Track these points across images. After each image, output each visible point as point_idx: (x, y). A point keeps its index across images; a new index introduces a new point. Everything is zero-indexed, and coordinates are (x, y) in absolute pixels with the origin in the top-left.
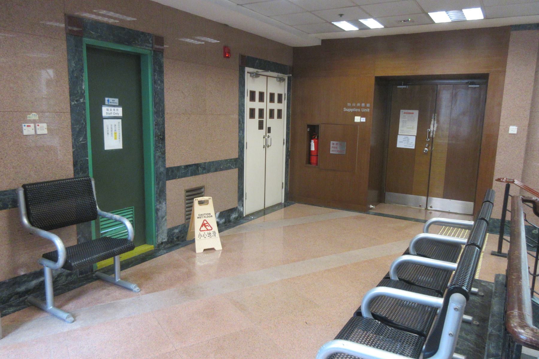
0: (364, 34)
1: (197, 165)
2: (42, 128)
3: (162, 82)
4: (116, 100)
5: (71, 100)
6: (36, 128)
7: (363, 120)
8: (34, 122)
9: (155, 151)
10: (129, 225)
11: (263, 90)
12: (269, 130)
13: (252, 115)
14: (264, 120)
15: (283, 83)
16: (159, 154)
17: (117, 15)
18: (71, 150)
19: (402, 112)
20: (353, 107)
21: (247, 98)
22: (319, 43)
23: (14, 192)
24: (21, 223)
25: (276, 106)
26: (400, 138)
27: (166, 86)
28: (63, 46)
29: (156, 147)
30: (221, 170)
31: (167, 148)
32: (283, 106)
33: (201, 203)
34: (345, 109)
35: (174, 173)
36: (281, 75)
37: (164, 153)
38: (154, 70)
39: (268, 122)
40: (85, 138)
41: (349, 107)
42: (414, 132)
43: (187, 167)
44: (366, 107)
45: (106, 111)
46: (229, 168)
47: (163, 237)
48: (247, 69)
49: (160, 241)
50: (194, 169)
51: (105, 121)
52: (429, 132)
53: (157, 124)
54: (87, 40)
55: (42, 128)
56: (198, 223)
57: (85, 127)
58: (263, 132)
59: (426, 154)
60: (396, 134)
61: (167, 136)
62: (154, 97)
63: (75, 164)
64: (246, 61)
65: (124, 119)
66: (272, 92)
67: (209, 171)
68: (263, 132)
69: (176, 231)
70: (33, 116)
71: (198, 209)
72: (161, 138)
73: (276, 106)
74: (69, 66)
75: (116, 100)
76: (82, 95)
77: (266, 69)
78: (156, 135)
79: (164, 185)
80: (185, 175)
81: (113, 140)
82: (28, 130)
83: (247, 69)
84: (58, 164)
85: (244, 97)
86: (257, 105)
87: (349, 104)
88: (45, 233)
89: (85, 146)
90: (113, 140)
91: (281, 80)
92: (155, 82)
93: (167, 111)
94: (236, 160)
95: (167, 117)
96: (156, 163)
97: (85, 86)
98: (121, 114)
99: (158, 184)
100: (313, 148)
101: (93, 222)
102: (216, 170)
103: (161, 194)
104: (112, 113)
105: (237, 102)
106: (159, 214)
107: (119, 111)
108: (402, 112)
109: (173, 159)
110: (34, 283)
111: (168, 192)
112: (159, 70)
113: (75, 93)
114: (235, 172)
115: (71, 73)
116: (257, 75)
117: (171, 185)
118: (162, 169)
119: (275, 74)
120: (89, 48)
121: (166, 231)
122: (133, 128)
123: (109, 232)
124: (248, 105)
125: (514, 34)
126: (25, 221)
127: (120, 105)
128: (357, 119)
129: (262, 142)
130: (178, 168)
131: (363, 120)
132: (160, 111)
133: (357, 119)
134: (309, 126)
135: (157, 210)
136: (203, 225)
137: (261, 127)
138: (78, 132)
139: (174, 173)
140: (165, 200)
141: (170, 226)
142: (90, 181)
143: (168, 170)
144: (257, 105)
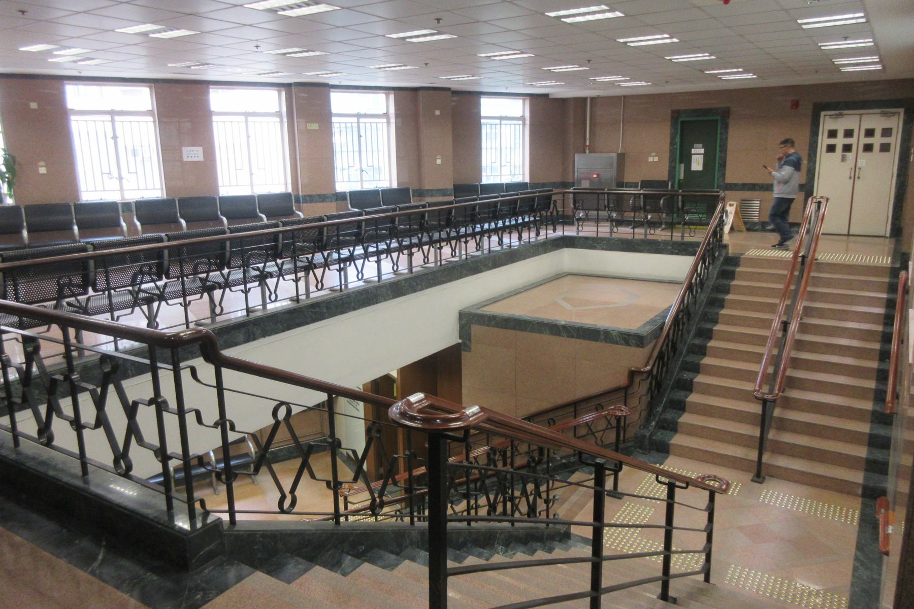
2: (656, 159)
3: (727, 133)
32: (895, 141)
37: (724, 174)
43: (744, 185)
45: (693, 151)
55: (656, 159)
64: (818, 109)
65: (705, 155)
70: (654, 154)
72: (723, 165)
76: (676, 144)
81: (697, 164)
82: (650, 159)
85: (817, 135)
90: (697, 164)
91: (884, 114)
92: (721, 134)
97: (678, 140)
107: (702, 151)
109: (730, 178)
112: (726, 126)
113: (672, 143)
116: (841, 115)
119: (879, 111)
124: (823, 141)
132: (724, 149)
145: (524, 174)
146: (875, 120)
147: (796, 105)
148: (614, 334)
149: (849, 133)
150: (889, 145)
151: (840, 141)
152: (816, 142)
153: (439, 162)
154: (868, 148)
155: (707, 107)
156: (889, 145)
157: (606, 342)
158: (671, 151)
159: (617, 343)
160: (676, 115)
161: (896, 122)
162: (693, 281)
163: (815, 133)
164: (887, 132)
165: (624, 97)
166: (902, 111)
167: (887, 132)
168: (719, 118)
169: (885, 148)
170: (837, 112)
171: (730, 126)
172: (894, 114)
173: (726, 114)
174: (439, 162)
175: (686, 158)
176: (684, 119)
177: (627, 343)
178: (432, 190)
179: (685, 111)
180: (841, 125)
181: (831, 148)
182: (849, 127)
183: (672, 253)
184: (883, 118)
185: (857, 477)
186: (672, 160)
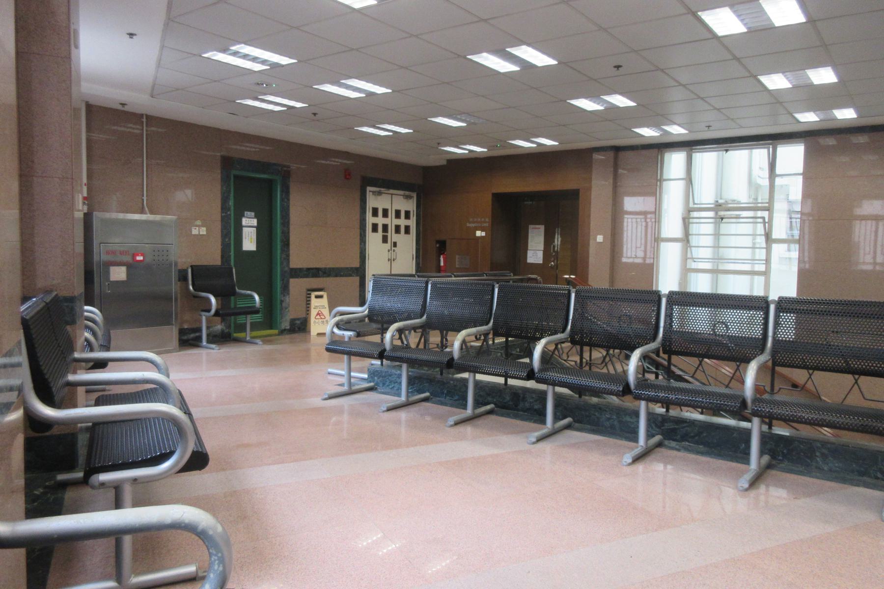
0: (472, 156)
1: (318, 269)
2: (203, 231)
3: (288, 200)
4: (253, 214)
5: (222, 212)
7: (483, 234)
8: (199, 226)
9: (282, 253)
10: (257, 297)
11: (388, 206)
12: (395, 244)
13: (375, 228)
14: (389, 234)
15: (411, 201)
16: (284, 256)
17: (257, 146)
18: (220, 247)
19: (531, 227)
20: (474, 222)
21: (369, 214)
22: (445, 163)
23: (186, 271)
24: (188, 288)
25: (402, 222)
26: (530, 254)
27: (291, 202)
28: (217, 175)
29: (283, 251)
30: (341, 276)
31: (291, 252)
32: (412, 223)
33: (317, 297)
34: (468, 225)
35: (298, 273)
36: (407, 193)
37: (288, 256)
38: (282, 191)
39: (392, 236)
40: (230, 239)
41: (470, 223)
42: (542, 247)
43: (308, 269)
44: (485, 222)
45: (245, 221)
46: (350, 275)
47: (286, 325)
48: (369, 189)
49: (283, 327)
50: (314, 272)
52: (554, 247)
53: (283, 232)
55: (203, 231)
56: (314, 312)
57: (231, 233)
58: (388, 246)
59: (552, 267)
60: (526, 249)
61: (291, 243)
62: (281, 211)
63: (222, 257)
64: (367, 181)
65: (259, 228)
66: (398, 208)
67: (329, 276)
68: (388, 246)
69: (298, 322)
70: (199, 223)
71: (314, 302)
72: (286, 244)
73: (402, 222)
74: (222, 189)
75: (253, 214)
76: (229, 209)
77: (389, 188)
78: (282, 241)
79: (288, 282)
80: (306, 276)
81: (249, 244)
82: (195, 231)
83: (369, 189)
84: (212, 257)
85: (365, 213)
86: (380, 220)
87: (471, 220)
88: (204, 294)
89: (229, 245)
90: (249, 244)
91: (408, 197)
93: (291, 222)
94: (357, 269)
95: (291, 227)
96: (282, 263)
97: (231, 203)
98: (256, 224)
99: (283, 280)
100: (442, 264)
101: (232, 298)
102: (336, 276)
103: (286, 288)
104: (249, 224)
105: (358, 217)
106: (284, 305)
107: (255, 222)
108: (531, 227)
109: (297, 261)
110: (192, 335)
111: (291, 288)
112: (286, 191)
113: (224, 208)
114: (357, 279)
115: (223, 194)
116: (380, 193)
117: (292, 281)
118: (286, 269)
120: (236, 177)
121: (289, 320)
122: (265, 234)
123: (241, 304)
124: (370, 220)
125: (597, 156)
126: (191, 288)
127: (256, 217)
128: (479, 233)
129: (386, 255)
130: (301, 269)
131: (483, 234)
132: (286, 223)
133: (479, 233)
134: (438, 242)
135: (282, 301)
136: (318, 314)
137: (385, 240)
138: (225, 235)
139: (298, 273)
140: (288, 294)
141: (292, 317)
142: (231, 269)
143: (292, 269)
144: (380, 220)
158: (223, 219)
160: (227, 163)
161: (410, 205)
162: (79, 425)
164: (407, 215)
166: (415, 195)
169: (407, 230)
171: (291, 190)
173: (286, 175)
181: (375, 228)
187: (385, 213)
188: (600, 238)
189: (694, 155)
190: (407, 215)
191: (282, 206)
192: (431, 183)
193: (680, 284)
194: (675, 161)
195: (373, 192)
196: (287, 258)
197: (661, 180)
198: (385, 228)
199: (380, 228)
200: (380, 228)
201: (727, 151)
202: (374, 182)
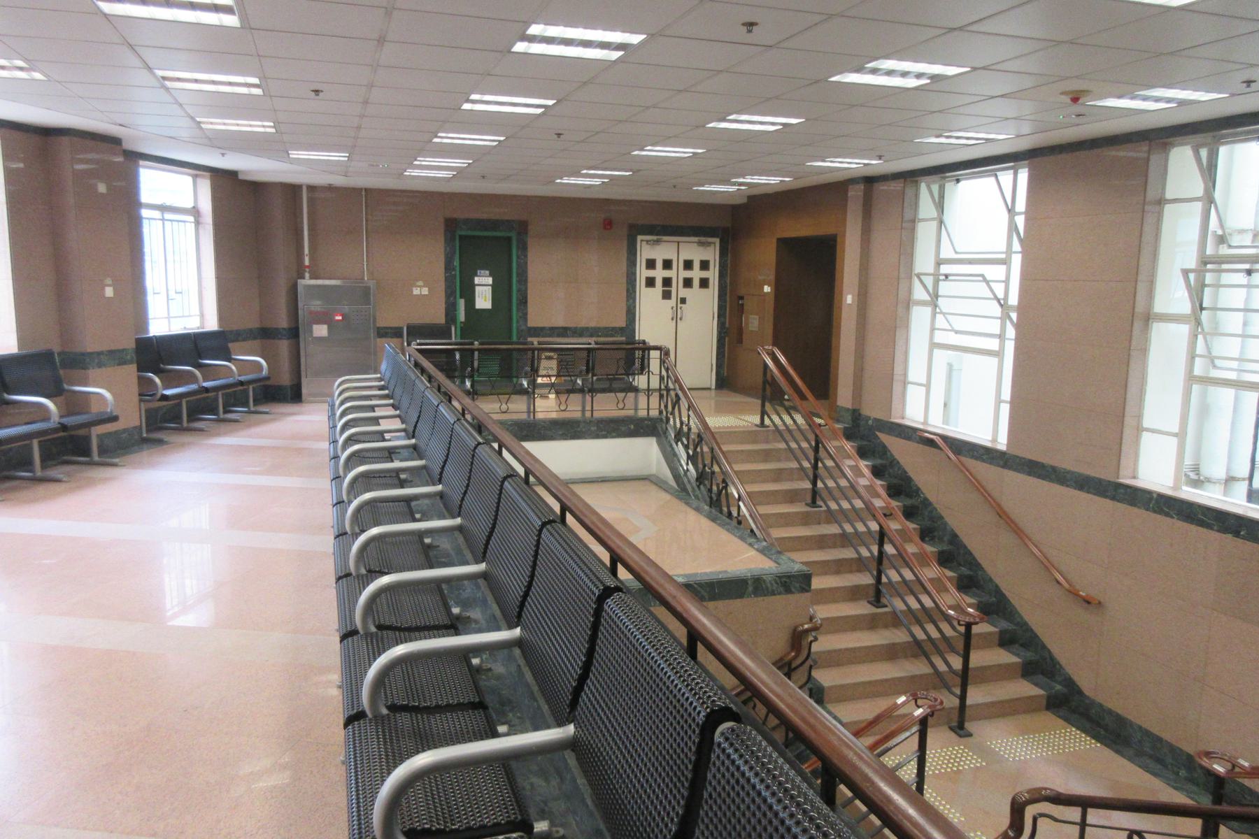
2: (425, 291)
3: (526, 256)
6: (420, 290)
12: (683, 301)
15: (711, 249)
22: (745, 200)
23: (401, 328)
28: (441, 239)
32: (713, 275)
36: (703, 239)
37: (526, 314)
38: (518, 248)
39: (678, 290)
45: (477, 280)
48: (640, 238)
51: (477, 288)
53: (519, 290)
54: (459, 233)
55: (425, 291)
58: (672, 302)
63: (447, 315)
64: (635, 230)
65: (495, 287)
68: (672, 302)
70: (420, 283)
72: (523, 302)
76: (454, 269)
81: (483, 301)
82: (416, 292)
83: (640, 238)
90: (483, 301)
91: (701, 244)
92: (518, 257)
94: (622, 329)
95: (529, 285)
97: (456, 263)
107: (490, 280)
112: (523, 248)
113: (448, 267)
116: (658, 242)
119: (696, 239)
120: (461, 237)
122: (500, 292)
124: (642, 273)
127: (491, 275)
129: (670, 314)
132: (523, 279)
137: (667, 295)
143: (530, 329)
145: (202, 315)
146: (692, 250)
147: (608, 224)
148: (768, 579)
149: (667, 264)
150: (648, 279)
151: (659, 273)
152: (635, 274)
153: (109, 292)
154: (688, 283)
155: (498, 217)
156: (648, 279)
157: (756, 595)
158: (446, 279)
159: (773, 594)
160: (451, 225)
161: (711, 254)
163: (632, 263)
165: (366, 190)
166: (717, 241)
167: (705, 265)
168: (513, 235)
169: (704, 283)
170: (655, 238)
172: (709, 244)
174: (109, 292)
175: (468, 292)
176: (463, 233)
177: (788, 590)
178: (99, 354)
179: (467, 221)
180: (661, 252)
181: (650, 282)
182: (667, 257)
183: (597, 437)
184: (701, 248)
185: (1026, 689)
186: (450, 294)
187: (667, 264)
188: (849, 299)
189: (1223, 150)
190: (705, 265)
191: (518, 265)
192: (730, 225)
193: (122, 362)
194: (1182, 164)
195: (647, 241)
196: (524, 316)
197: (914, 221)
198: (667, 282)
199: (659, 282)
200: (659, 282)
201: (958, 181)
202: (651, 230)
